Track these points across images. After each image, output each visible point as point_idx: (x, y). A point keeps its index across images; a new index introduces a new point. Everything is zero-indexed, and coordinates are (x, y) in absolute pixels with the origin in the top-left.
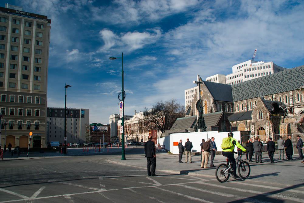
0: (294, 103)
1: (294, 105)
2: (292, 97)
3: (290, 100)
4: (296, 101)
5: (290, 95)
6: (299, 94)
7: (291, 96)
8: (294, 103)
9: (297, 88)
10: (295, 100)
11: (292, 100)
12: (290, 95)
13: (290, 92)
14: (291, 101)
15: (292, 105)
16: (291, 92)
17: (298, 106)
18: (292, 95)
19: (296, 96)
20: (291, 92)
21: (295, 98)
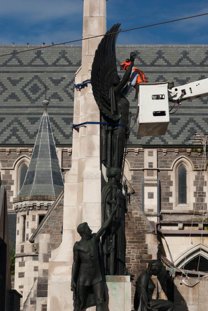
0: (163, 211)
1: (167, 219)
2: (156, 177)
3: (147, 190)
4: (173, 200)
5: (146, 166)
6: (189, 167)
7: (150, 170)
8: (163, 211)
9: (180, 141)
10: (170, 194)
11: (155, 190)
12: (146, 166)
13: (147, 151)
14: (151, 196)
15: (155, 220)
16: (155, 151)
17: (185, 225)
18: (155, 166)
19: (173, 176)
20: (151, 154)
21: (171, 183)
